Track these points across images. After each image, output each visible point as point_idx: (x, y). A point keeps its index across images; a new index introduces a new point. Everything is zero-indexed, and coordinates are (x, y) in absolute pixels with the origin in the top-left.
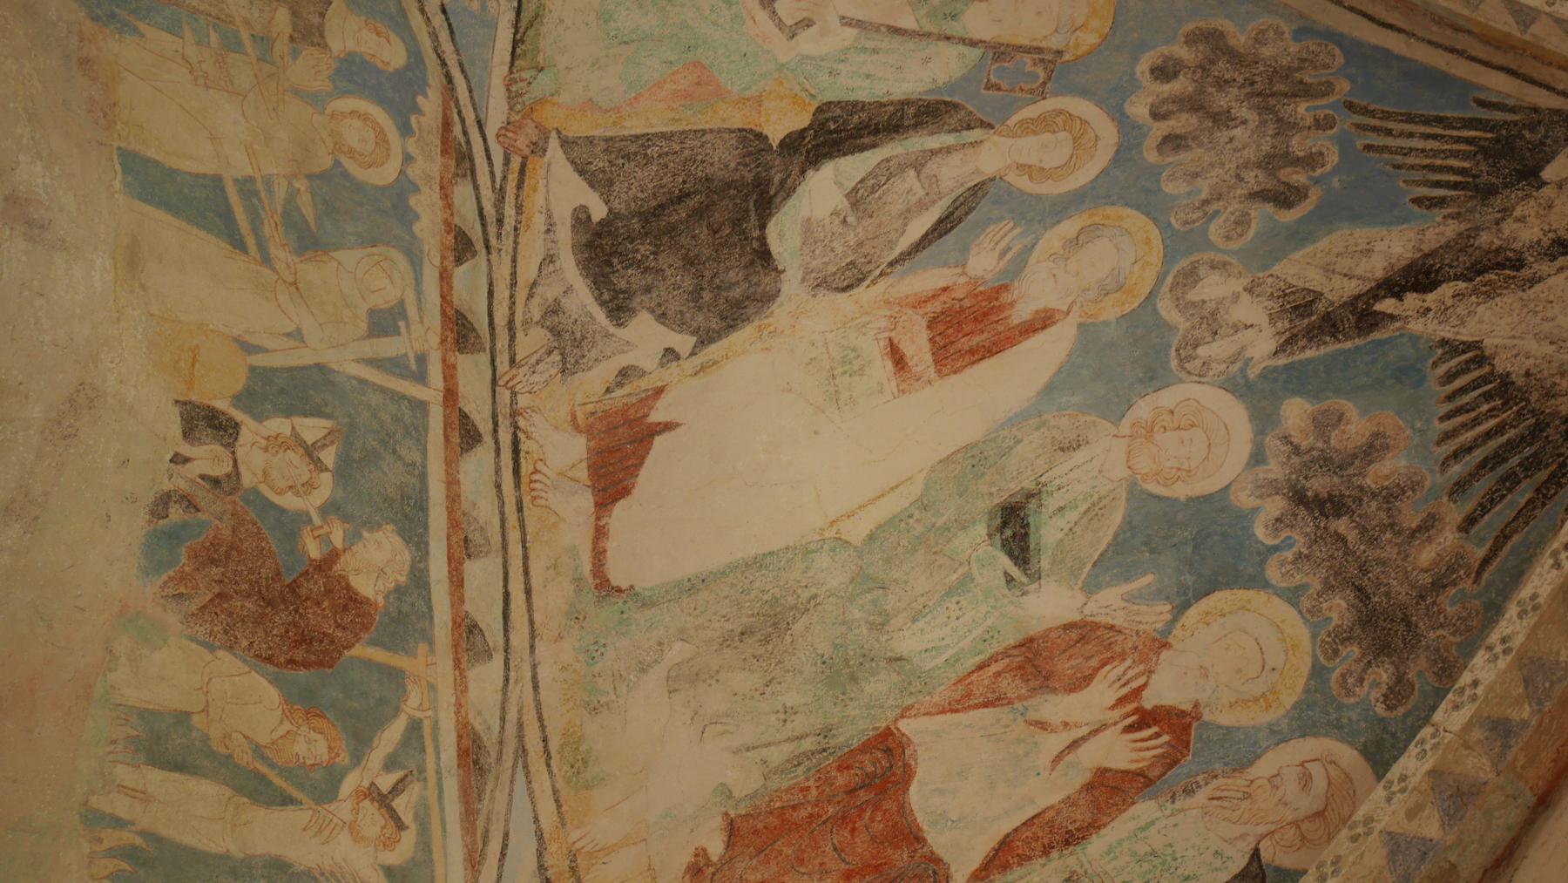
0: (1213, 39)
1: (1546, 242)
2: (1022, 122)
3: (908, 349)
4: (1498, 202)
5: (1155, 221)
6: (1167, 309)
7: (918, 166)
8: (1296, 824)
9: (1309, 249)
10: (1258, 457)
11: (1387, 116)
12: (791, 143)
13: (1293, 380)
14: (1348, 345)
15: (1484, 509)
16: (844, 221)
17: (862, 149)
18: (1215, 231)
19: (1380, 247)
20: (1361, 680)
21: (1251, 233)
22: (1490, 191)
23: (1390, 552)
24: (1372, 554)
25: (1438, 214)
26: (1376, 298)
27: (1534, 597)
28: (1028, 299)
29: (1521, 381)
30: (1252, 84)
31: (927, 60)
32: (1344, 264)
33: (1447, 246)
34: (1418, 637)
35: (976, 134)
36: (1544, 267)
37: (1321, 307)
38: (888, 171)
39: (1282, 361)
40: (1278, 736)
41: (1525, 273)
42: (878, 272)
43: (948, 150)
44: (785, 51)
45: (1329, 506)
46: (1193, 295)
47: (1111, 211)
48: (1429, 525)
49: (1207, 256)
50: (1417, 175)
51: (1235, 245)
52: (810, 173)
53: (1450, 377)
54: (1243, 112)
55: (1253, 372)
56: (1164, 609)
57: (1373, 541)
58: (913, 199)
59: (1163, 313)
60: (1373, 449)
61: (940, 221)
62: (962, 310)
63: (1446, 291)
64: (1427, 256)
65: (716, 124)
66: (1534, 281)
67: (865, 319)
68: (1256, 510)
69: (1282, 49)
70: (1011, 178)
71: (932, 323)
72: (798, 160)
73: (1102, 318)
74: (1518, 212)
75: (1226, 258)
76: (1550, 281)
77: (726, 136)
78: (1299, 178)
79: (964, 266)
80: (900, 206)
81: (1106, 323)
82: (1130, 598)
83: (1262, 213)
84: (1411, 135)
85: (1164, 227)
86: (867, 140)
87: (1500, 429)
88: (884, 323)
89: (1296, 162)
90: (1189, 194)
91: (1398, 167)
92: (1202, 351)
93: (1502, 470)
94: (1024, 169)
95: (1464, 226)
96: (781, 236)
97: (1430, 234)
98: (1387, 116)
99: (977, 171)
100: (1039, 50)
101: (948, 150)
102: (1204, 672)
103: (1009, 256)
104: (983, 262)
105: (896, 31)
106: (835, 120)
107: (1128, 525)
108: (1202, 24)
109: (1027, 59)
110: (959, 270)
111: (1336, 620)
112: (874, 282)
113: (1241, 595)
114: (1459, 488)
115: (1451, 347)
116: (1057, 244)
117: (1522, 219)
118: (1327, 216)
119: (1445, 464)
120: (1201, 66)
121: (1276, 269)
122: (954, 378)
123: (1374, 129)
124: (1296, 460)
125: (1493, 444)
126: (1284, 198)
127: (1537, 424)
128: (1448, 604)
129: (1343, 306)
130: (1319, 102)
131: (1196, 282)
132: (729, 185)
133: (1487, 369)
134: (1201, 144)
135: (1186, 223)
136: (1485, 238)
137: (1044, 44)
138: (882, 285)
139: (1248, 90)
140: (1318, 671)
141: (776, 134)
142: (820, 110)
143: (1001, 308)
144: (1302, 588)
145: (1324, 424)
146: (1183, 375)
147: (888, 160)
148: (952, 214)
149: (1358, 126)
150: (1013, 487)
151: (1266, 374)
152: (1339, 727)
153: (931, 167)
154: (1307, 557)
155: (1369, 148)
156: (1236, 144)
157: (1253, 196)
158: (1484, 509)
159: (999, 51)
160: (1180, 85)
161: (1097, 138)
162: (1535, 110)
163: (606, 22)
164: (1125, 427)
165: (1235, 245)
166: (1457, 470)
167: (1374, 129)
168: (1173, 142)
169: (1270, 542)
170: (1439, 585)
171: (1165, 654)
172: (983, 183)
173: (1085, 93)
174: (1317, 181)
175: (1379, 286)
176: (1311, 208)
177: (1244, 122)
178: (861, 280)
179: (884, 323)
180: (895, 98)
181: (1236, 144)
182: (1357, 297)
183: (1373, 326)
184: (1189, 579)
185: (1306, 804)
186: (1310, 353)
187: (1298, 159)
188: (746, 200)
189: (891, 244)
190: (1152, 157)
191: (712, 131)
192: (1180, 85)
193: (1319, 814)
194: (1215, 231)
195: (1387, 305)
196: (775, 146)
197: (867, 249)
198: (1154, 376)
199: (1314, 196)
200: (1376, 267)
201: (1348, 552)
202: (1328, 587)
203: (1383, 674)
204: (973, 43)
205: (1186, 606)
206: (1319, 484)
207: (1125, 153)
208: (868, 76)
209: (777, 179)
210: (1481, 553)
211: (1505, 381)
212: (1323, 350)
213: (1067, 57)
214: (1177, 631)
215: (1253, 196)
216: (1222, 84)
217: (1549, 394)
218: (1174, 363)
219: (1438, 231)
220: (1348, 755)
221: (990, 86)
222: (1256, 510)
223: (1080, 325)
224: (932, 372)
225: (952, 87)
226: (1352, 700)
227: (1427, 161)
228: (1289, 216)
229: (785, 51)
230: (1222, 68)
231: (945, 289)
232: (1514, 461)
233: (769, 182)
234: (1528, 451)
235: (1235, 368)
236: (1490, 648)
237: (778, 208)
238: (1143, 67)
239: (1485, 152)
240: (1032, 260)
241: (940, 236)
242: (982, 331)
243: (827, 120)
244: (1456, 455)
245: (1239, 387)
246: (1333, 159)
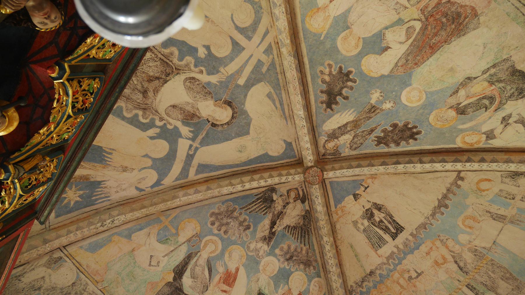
0: (213, 214)
1: (282, 207)
2: (203, 247)
3: (224, 289)
4: (272, 207)
5: (236, 245)
6: (250, 254)
7: (196, 265)
8: (319, 291)
9: (258, 231)
10: (279, 260)
11: (247, 206)
12: (175, 279)
13: (273, 248)
14: (274, 238)
15: (305, 242)
16: (195, 282)
17: (186, 270)
18: (245, 239)
19: (265, 224)
20: (310, 271)
21: (249, 235)
22: (270, 207)
23: (301, 256)
24: (299, 258)
25: (267, 214)
26: (272, 230)
27: (328, 250)
28: (232, 268)
29: (295, 225)
30: (226, 216)
31: (181, 251)
32: (264, 229)
33: (272, 217)
34: (311, 261)
35: (199, 254)
36: (285, 210)
37: (267, 237)
38: (193, 270)
39: (270, 247)
40: (309, 285)
41: (284, 213)
42: (209, 284)
43: (198, 259)
44: (160, 269)
45: (291, 257)
46: (251, 249)
47: (229, 248)
48: (302, 250)
49: (247, 243)
50: (260, 211)
51: (249, 239)
52: (182, 280)
53: (288, 231)
54: (229, 221)
55: (268, 251)
56: (286, 286)
57: (298, 256)
58: (201, 270)
59: (251, 255)
60: (289, 247)
61: (209, 270)
62: (226, 278)
63: (278, 222)
64: (271, 220)
65: (161, 287)
66: (286, 213)
67: (214, 291)
68: (285, 266)
69: (223, 208)
70: (211, 255)
71: (224, 283)
72: (178, 280)
73: (244, 262)
74: (276, 206)
75: (250, 241)
76: (287, 211)
77: (164, 287)
78: (246, 223)
79: (219, 272)
80: (200, 273)
81: (245, 262)
82: (282, 289)
83: (247, 232)
84: (253, 207)
85: (239, 244)
86: (185, 269)
87: (298, 232)
88: (218, 289)
89: (243, 222)
90: (236, 237)
91: (257, 212)
92: (260, 255)
93: (303, 236)
94: (211, 253)
95: (272, 213)
96: (188, 292)
97: (269, 217)
98: (247, 206)
99: (205, 259)
100: (194, 236)
101: (198, 259)
102: (297, 287)
103: (223, 266)
104: (221, 270)
105: (172, 251)
106: (177, 270)
107: (274, 282)
108: (210, 213)
109: (194, 238)
110: (219, 274)
111: (303, 268)
112: (210, 286)
113: (292, 276)
114: (301, 242)
115: (285, 228)
116: (228, 259)
117: (277, 207)
118: (255, 226)
119: (297, 241)
120: (216, 219)
121: (257, 237)
122: (234, 286)
123: (247, 209)
124: (283, 256)
125: (300, 234)
126: (248, 227)
127: (301, 228)
128: (310, 254)
129: (269, 235)
130: (237, 211)
131: (250, 247)
132: (172, 292)
133: (291, 227)
134: (229, 229)
135: (241, 241)
136: (276, 213)
137: (193, 234)
138: (211, 285)
139: (226, 217)
140: (306, 275)
141: (171, 280)
142: (173, 271)
143: (230, 273)
144: (297, 269)
145: (282, 249)
146: (261, 260)
147: (191, 268)
148: (209, 267)
149: (245, 211)
150: (256, 291)
151: (270, 251)
152: (313, 277)
153: (198, 264)
154: (294, 265)
155: (250, 212)
156: (234, 226)
157: (244, 231)
158: (305, 242)
159: (189, 241)
160: (217, 224)
161: (215, 240)
162: (263, 192)
163: (129, 291)
164: (261, 272)
165: (249, 239)
166: (299, 241)
167: (247, 209)
168: (226, 232)
169: (289, 267)
170: (308, 254)
171: (291, 290)
172: (208, 259)
173: (206, 236)
174: (249, 222)
175: (270, 229)
176: (252, 227)
177: (231, 222)
178: (208, 287)
179: (218, 289)
180: (182, 260)
181: (234, 226)
182: (270, 232)
183: (275, 234)
184: (286, 280)
185: (318, 288)
186: (272, 243)
187: (243, 221)
188: (177, 292)
189: (206, 279)
190: (226, 237)
191: (161, 289)
192: (217, 224)
193: (319, 287)
194: (245, 239)
195: (274, 230)
196: (172, 281)
197: (203, 282)
198: (258, 263)
199: (251, 224)
200: (268, 227)
201: (297, 260)
202: (299, 265)
203: (312, 268)
204: (184, 243)
205: (288, 283)
206: (288, 256)
207: (221, 239)
208: (175, 261)
209: (178, 285)
210: (308, 246)
211: (294, 227)
212: (273, 242)
213: (198, 233)
214: (290, 286)
215: (244, 231)
216: (222, 219)
217: (299, 224)
218: (258, 259)
219: (270, 216)
220: (316, 279)
221: (193, 246)
222: (285, 266)
223: (242, 265)
224: (231, 289)
225: (188, 251)
226: (311, 274)
227: (259, 209)
228: (251, 229)
229: (160, 269)
230: (219, 217)
231: (221, 277)
232: (303, 234)
233: (177, 287)
234: (303, 232)
235: (266, 253)
236: (329, 259)
237: (183, 288)
238: (209, 225)
239: (264, 202)
240: (227, 263)
241: (211, 271)
242: (231, 278)
243: (176, 271)
244: (297, 239)
245: (269, 254)
246: (247, 217)
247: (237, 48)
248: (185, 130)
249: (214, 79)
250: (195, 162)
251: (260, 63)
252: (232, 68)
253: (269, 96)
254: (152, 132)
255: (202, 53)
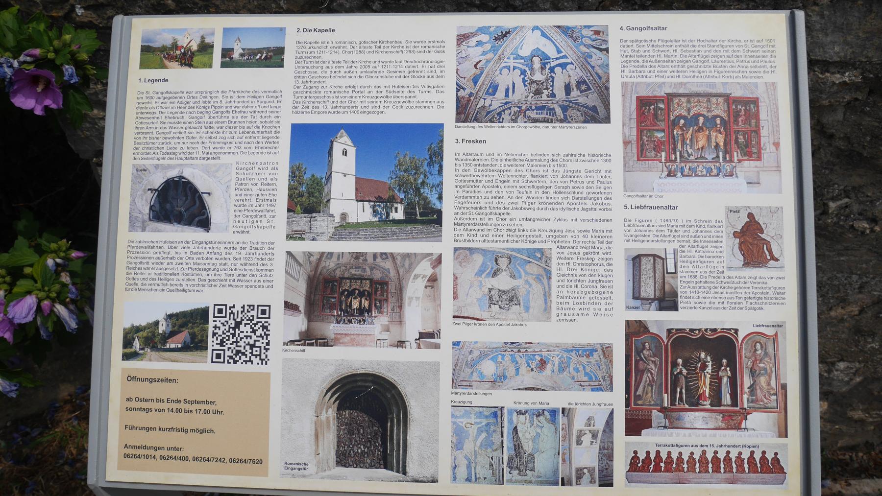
247: (514, 68)
248: (548, 66)
249: (527, 69)
250: (558, 56)
251: (514, 59)
252: (521, 66)
253: (521, 49)
254: (553, 75)
255: (522, 76)
